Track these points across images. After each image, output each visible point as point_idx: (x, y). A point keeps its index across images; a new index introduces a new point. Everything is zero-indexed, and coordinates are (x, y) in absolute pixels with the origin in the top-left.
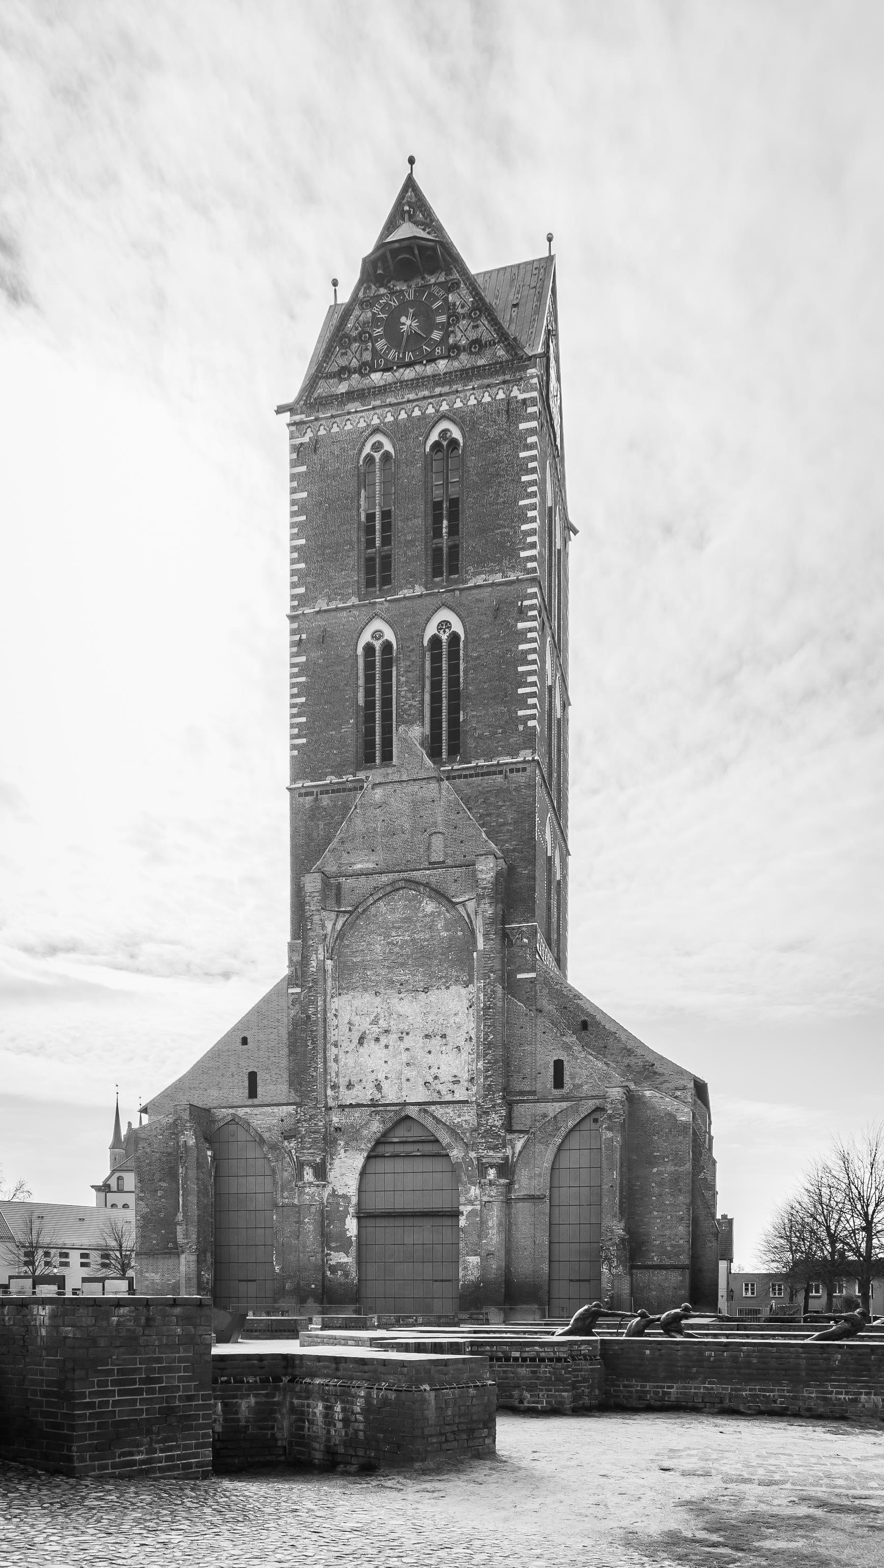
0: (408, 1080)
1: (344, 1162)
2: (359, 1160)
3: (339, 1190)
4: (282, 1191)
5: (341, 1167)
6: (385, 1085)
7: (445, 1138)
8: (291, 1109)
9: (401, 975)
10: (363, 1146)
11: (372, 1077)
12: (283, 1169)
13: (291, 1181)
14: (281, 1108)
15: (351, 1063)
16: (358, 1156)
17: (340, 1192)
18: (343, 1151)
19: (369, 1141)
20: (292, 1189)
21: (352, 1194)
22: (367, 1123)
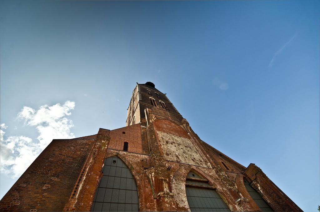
0: (186, 157)
1: (177, 186)
2: (183, 187)
3: (179, 204)
4: (146, 203)
5: (176, 189)
6: (180, 157)
7: (210, 179)
8: (146, 157)
9: (172, 132)
10: (182, 179)
11: (174, 154)
12: (145, 187)
13: (151, 195)
14: (142, 155)
15: (165, 148)
16: (182, 184)
17: (181, 205)
18: (174, 180)
19: (184, 177)
20: (152, 201)
21: (187, 207)
22: (180, 169)
